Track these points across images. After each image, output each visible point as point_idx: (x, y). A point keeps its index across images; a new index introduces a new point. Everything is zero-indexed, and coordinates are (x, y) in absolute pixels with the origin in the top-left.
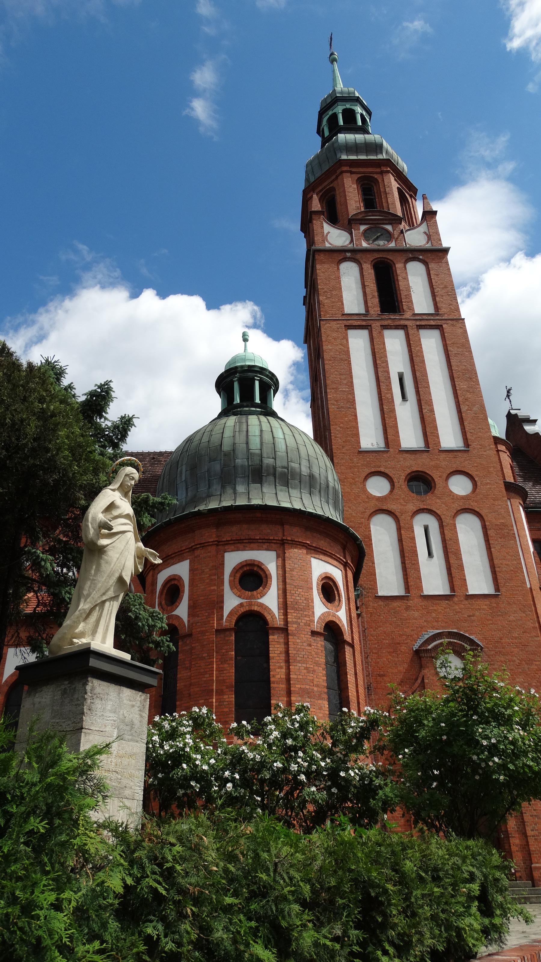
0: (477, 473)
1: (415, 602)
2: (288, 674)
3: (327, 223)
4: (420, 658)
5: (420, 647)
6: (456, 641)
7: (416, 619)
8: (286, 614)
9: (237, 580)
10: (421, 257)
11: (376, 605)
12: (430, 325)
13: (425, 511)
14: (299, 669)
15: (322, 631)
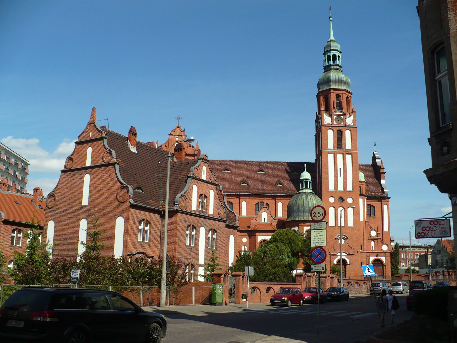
10: (350, 129)
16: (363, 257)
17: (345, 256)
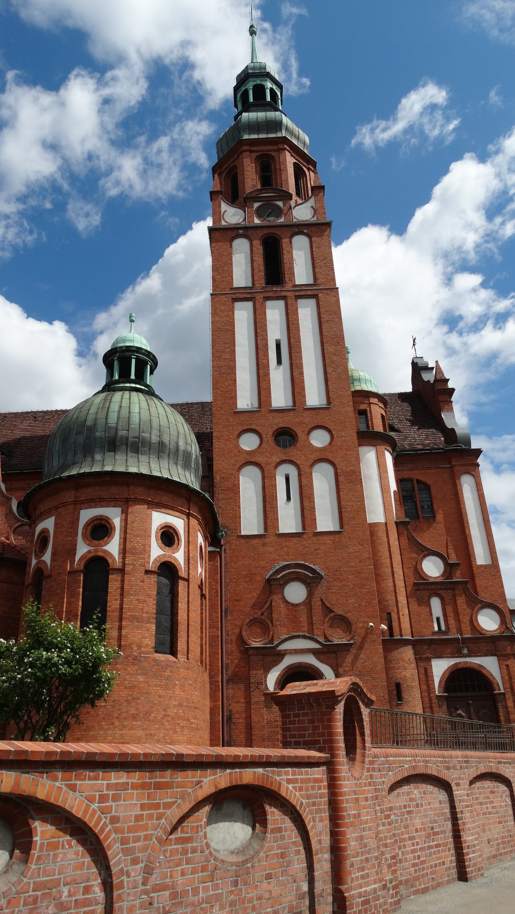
0: (335, 427)
1: (271, 539)
2: (121, 605)
3: (225, 202)
4: (271, 585)
5: (270, 576)
6: (300, 571)
7: (270, 553)
8: (124, 558)
9: (88, 532)
10: (305, 231)
11: (238, 543)
12: (307, 295)
13: (287, 462)
14: (131, 600)
15: (156, 570)
16: (403, 660)
17: (315, 652)
